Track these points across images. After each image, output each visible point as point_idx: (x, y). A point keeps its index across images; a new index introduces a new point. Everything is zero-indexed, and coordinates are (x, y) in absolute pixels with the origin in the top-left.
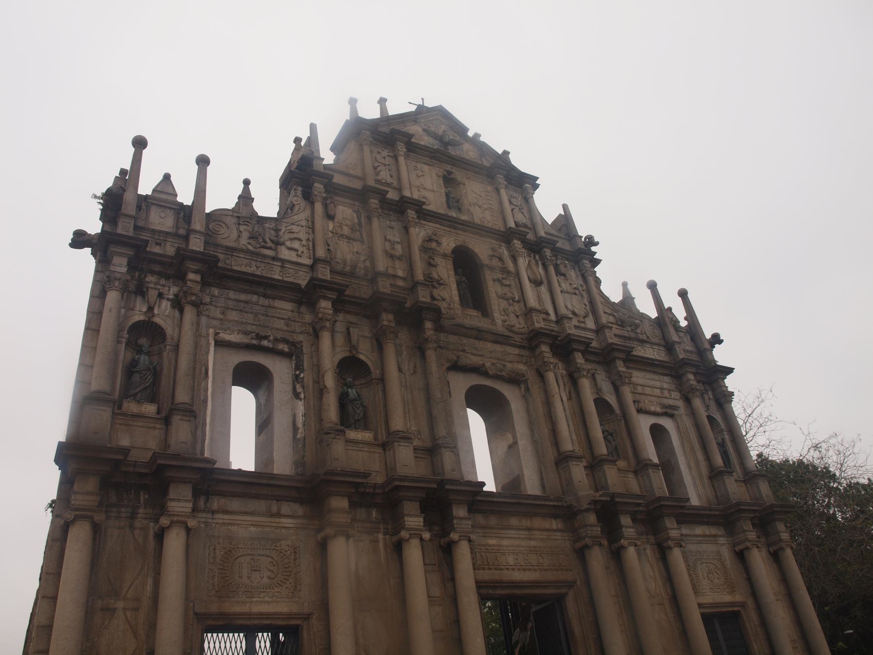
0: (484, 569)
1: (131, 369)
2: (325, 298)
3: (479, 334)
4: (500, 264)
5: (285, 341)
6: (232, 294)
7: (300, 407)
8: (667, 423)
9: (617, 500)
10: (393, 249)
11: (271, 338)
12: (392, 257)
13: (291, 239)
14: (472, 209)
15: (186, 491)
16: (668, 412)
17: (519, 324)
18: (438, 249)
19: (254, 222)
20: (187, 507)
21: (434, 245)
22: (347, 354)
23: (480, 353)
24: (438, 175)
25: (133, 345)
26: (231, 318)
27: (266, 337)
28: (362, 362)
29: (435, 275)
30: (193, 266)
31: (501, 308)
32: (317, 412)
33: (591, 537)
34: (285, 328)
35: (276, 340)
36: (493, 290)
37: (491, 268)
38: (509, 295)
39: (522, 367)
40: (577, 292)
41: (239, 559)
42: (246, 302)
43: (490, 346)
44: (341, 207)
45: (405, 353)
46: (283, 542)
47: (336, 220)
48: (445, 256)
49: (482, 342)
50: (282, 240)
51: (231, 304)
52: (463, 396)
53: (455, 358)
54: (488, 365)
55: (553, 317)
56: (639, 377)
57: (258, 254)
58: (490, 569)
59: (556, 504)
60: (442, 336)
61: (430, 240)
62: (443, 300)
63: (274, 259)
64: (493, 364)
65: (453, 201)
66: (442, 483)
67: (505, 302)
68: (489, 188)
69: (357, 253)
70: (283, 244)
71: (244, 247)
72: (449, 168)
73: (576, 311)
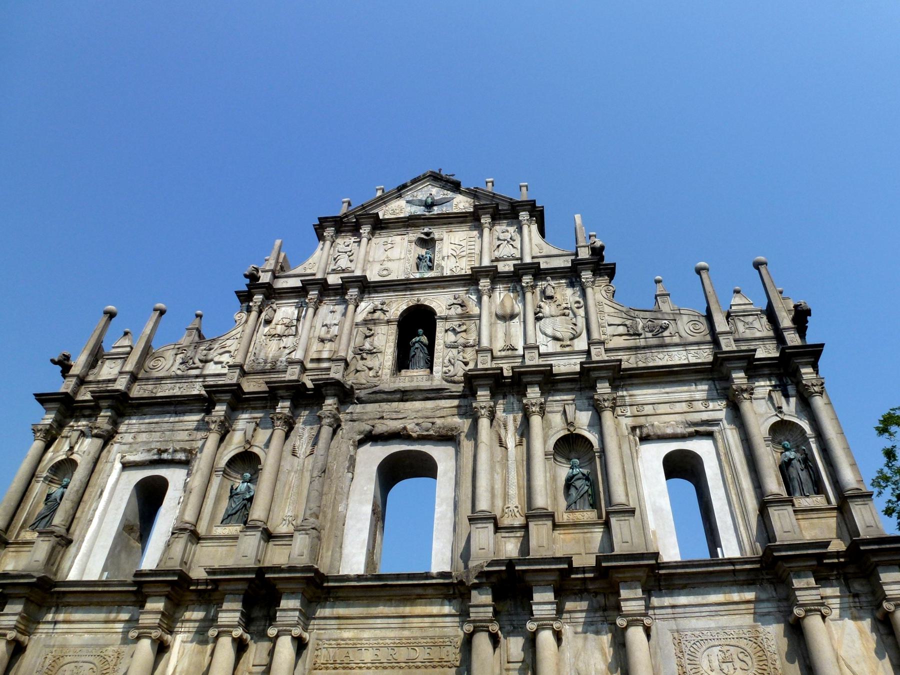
0: (327, 668)
2: (221, 401)
3: (405, 395)
4: (459, 310)
5: (184, 450)
8: (702, 448)
9: (517, 568)
10: (328, 332)
11: (171, 451)
12: (322, 340)
13: (221, 354)
14: (443, 264)
17: (459, 371)
18: (382, 316)
19: (192, 348)
21: (378, 314)
22: (241, 450)
23: (401, 416)
24: (410, 242)
26: (139, 440)
27: (166, 451)
28: (254, 453)
29: (367, 346)
30: (104, 403)
31: (447, 358)
32: (182, 512)
33: (474, 621)
34: (187, 438)
35: (175, 451)
37: (446, 319)
38: (461, 341)
40: (567, 311)
41: (64, 667)
42: (157, 423)
43: (418, 405)
44: (283, 309)
45: (306, 435)
46: (110, 648)
47: (274, 322)
48: (388, 322)
49: (408, 405)
50: (210, 357)
51: (143, 427)
52: (375, 468)
53: (368, 428)
54: (409, 427)
55: (520, 352)
57: (182, 377)
58: (335, 668)
59: (441, 581)
60: (358, 408)
61: (374, 311)
62: (370, 369)
63: (197, 376)
64: (417, 424)
67: (455, 351)
68: (475, 233)
69: (284, 347)
70: (212, 360)
71: (173, 374)
72: (426, 230)
73: (559, 335)
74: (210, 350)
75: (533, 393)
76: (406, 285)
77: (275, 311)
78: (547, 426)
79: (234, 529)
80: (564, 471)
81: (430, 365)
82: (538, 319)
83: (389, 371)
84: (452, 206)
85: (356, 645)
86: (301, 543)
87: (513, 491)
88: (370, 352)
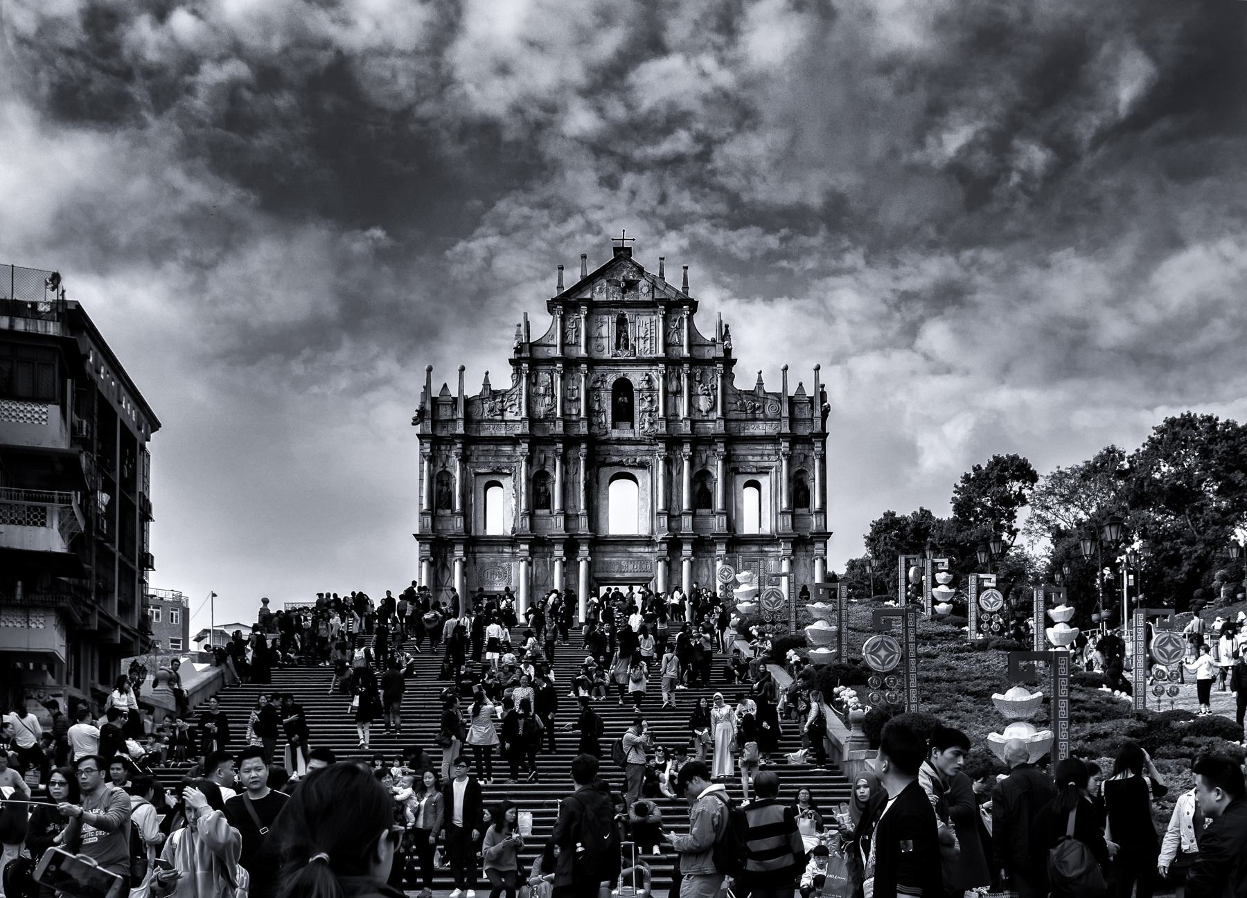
1: (440, 492)
3: (620, 441)
6: (481, 448)
7: (514, 501)
15: (461, 547)
16: (764, 471)
20: (461, 553)
25: (440, 482)
29: (597, 407)
36: (640, 406)
37: (640, 391)
39: (648, 458)
43: (627, 448)
49: (622, 448)
56: (741, 450)
63: (502, 421)
65: (622, 340)
66: (571, 536)
68: (654, 318)
74: (502, 402)
75: (687, 449)
76: (616, 363)
77: (537, 377)
78: (692, 466)
79: (546, 512)
80: (698, 487)
81: (630, 419)
82: (690, 396)
83: (609, 425)
84: (637, 290)
85: (610, 563)
86: (583, 522)
87: (674, 498)
88: (599, 412)
